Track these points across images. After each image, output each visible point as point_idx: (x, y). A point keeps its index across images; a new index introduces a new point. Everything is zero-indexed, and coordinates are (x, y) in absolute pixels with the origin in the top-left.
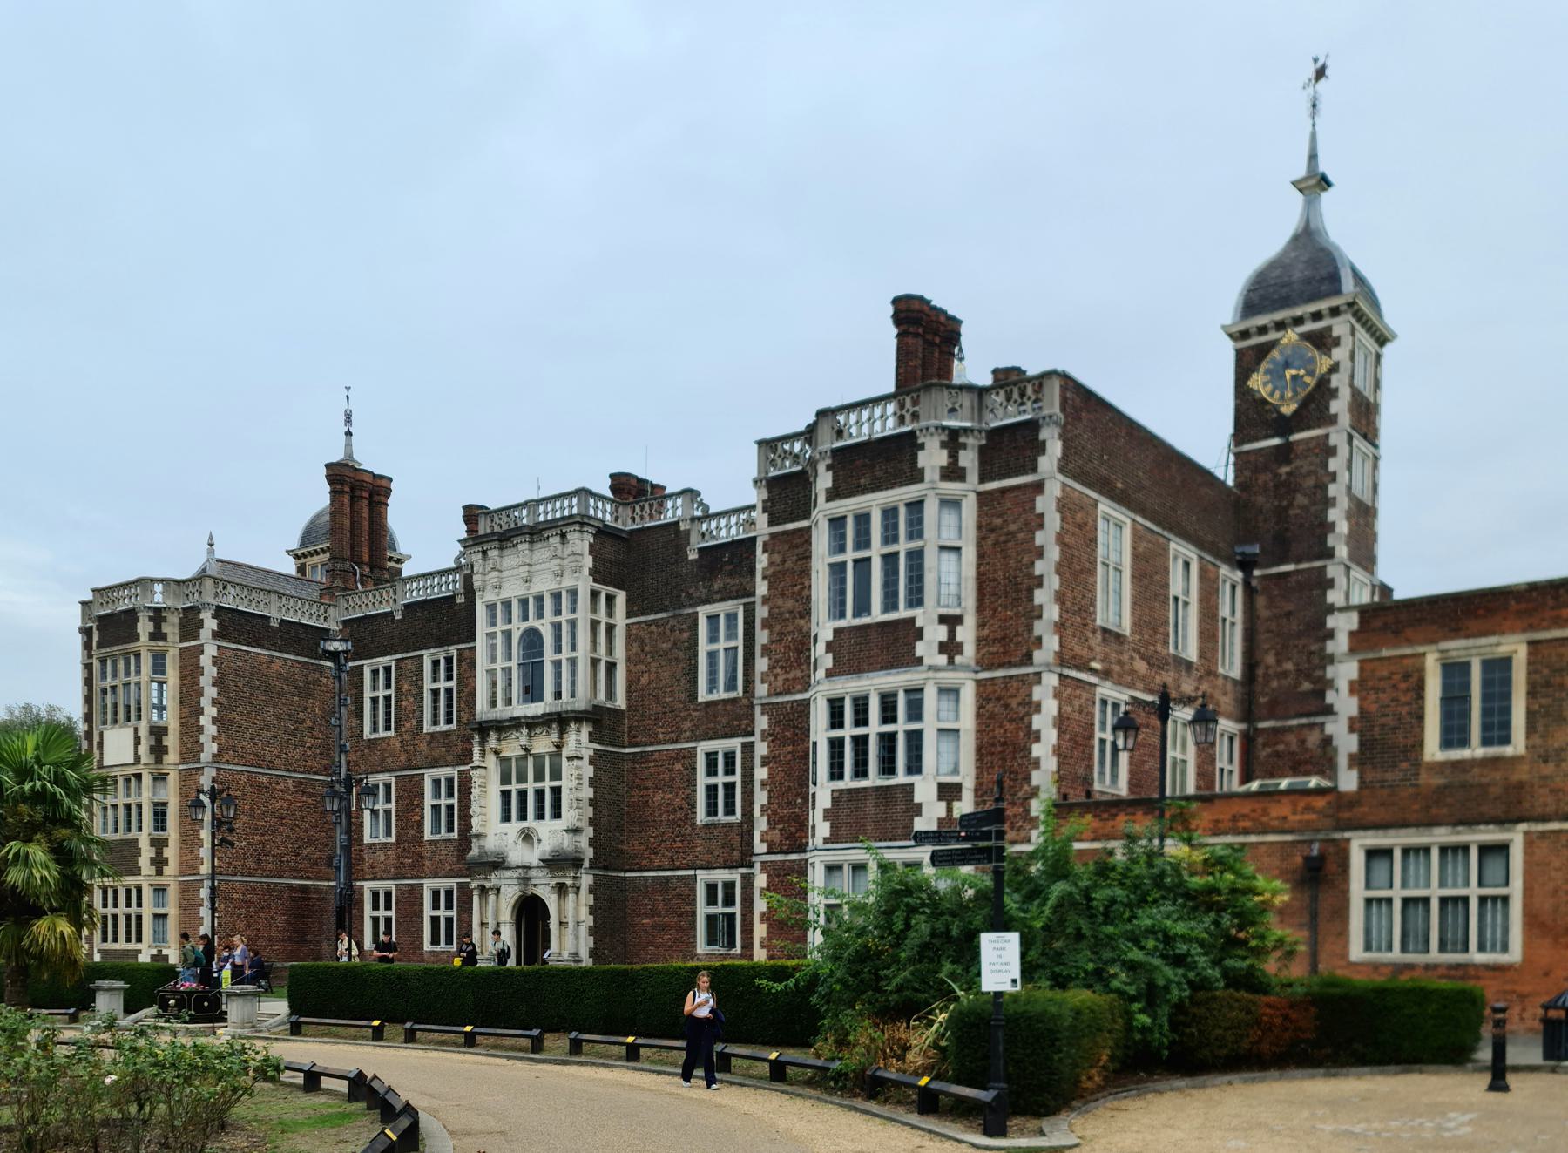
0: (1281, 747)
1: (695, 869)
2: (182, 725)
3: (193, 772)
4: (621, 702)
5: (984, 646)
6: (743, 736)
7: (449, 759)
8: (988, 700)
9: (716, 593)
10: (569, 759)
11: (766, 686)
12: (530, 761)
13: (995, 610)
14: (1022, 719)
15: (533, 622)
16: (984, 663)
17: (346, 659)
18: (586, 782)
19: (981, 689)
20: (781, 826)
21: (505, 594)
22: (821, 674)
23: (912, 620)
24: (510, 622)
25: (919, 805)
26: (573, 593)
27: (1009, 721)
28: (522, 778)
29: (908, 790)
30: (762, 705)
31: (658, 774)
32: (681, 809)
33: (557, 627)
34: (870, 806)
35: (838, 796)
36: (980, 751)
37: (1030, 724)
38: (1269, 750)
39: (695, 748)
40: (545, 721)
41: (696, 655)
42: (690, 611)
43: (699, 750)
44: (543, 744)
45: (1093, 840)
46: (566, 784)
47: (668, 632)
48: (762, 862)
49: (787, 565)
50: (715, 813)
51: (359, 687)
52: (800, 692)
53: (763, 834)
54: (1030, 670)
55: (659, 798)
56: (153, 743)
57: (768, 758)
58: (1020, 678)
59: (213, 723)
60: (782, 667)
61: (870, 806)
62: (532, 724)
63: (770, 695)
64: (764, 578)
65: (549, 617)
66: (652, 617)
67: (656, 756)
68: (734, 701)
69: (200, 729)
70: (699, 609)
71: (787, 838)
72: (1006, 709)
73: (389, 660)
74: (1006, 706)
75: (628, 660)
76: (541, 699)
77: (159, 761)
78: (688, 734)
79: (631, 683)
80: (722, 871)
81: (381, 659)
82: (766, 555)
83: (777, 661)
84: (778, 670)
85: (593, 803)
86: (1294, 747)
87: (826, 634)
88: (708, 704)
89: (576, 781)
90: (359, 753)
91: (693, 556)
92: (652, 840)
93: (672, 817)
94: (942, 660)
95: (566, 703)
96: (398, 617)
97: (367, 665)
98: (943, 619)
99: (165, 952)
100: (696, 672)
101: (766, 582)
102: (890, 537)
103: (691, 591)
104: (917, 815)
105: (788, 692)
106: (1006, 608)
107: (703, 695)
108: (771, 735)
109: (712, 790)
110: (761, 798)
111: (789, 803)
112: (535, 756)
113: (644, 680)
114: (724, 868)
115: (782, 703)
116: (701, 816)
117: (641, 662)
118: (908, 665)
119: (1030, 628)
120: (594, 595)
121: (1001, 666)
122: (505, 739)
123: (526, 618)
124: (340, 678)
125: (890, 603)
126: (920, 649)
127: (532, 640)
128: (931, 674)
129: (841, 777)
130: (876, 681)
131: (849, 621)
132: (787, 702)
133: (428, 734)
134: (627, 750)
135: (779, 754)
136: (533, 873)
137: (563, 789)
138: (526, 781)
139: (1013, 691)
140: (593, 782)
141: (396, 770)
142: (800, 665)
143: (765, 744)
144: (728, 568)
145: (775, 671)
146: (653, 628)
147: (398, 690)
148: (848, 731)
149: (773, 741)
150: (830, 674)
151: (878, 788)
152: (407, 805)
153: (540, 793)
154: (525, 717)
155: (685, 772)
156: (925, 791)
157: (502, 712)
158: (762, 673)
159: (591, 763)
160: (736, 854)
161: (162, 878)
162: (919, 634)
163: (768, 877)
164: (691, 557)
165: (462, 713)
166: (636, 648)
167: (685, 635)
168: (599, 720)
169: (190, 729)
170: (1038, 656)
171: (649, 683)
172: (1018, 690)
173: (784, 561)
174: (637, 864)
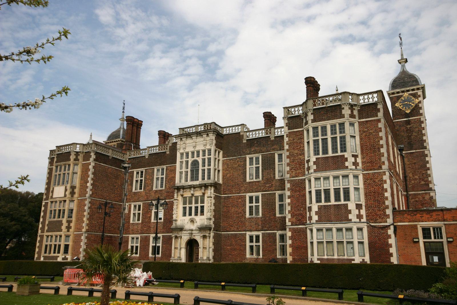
0: (417, 199)
1: (246, 231)
2: (81, 186)
3: (83, 200)
4: (221, 182)
5: (365, 164)
8: (367, 179)
10: (208, 197)
11: (289, 175)
12: (194, 198)
13: (367, 154)
14: (380, 185)
15: (195, 158)
16: (364, 169)
17: (129, 169)
18: (213, 204)
19: (365, 176)
20: (296, 217)
21: (187, 150)
23: (344, 155)
24: (188, 158)
25: (350, 210)
26: (210, 150)
27: (375, 186)
28: (191, 203)
29: (346, 206)
30: (288, 180)
32: (241, 213)
33: (204, 160)
34: (332, 210)
35: (320, 208)
36: (366, 195)
38: (413, 200)
39: (246, 195)
40: (200, 186)
41: (246, 168)
42: (244, 156)
43: (247, 196)
44: (198, 193)
46: (206, 205)
47: (236, 162)
48: (289, 228)
50: (252, 215)
51: (132, 177)
52: (301, 177)
53: (289, 219)
54: (381, 171)
55: (233, 209)
57: (290, 196)
58: (378, 173)
59: (91, 185)
60: (294, 169)
61: (332, 210)
62: (194, 187)
63: (290, 177)
64: (287, 144)
65: (201, 156)
66: (231, 158)
68: (259, 182)
70: (247, 156)
71: (298, 221)
72: (374, 182)
73: (143, 170)
74: (374, 181)
75: (223, 170)
76: (198, 180)
77: (72, 196)
78: (243, 191)
79: (223, 176)
82: (288, 138)
85: (214, 211)
86: (421, 199)
87: (313, 159)
88: (250, 182)
89: (209, 204)
90: (131, 196)
91: (245, 141)
94: (354, 167)
95: (206, 181)
96: (147, 157)
97: (135, 171)
98: (353, 156)
99: (67, 257)
100: (246, 173)
101: (288, 145)
102: (333, 131)
104: (349, 214)
105: (297, 176)
106: (371, 153)
107: (248, 180)
108: (291, 189)
109: (251, 208)
110: (288, 208)
111: (298, 210)
112: (195, 197)
113: (228, 175)
115: (295, 180)
116: (248, 215)
117: (227, 170)
119: (380, 159)
120: (216, 151)
121: (371, 170)
122: (185, 191)
123: (193, 157)
124: (126, 174)
125: (335, 150)
126: (347, 164)
127: (195, 164)
128: (351, 171)
129: (321, 202)
130: (332, 173)
132: (297, 179)
133: (155, 190)
134: (222, 196)
135: (294, 195)
136: (194, 232)
137: (205, 206)
138: (192, 204)
140: (214, 204)
141: (143, 201)
142: (300, 169)
143: (289, 192)
144: (256, 145)
145: (292, 171)
146: (231, 161)
147: (145, 178)
149: (292, 191)
151: (335, 205)
153: (196, 208)
154: (194, 185)
156: (351, 206)
157: (183, 183)
158: (287, 171)
159: (214, 199)
160: (260, 227)
161: (69, 233)
162: (346, 160)
163: (292, 233)
164: (244, 142)
165: (167, 185)
166: (226, 166)
167: (242, 163)
168: (216, 186)
169: (83, 187)
170: (383, 167)
172: (378, 177)
173: (294, 140)
174: (225, 230)
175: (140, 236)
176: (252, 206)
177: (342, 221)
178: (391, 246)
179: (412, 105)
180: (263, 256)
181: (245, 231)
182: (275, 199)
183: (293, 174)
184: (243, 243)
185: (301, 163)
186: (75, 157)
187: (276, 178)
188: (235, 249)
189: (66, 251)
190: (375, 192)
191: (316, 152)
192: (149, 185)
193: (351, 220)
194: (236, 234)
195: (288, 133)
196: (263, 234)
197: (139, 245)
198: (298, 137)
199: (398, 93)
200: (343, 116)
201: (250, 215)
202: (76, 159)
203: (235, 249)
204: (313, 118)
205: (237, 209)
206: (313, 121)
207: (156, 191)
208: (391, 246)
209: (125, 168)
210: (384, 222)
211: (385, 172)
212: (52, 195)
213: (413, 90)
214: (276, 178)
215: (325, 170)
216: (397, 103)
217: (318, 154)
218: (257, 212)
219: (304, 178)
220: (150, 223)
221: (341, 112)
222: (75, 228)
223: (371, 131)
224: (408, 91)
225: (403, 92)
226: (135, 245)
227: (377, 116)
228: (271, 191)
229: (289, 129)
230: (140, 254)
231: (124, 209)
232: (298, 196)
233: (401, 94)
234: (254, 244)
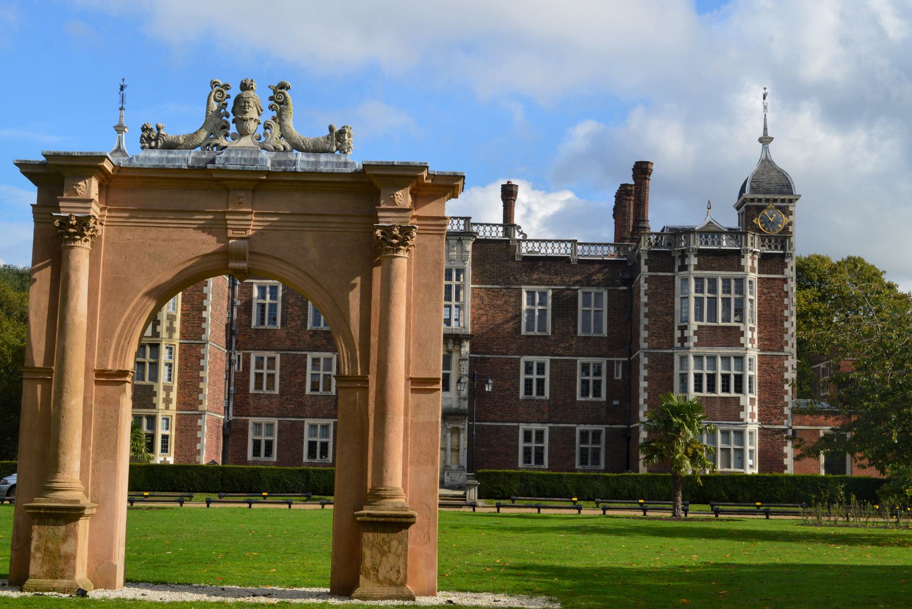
1: (519, 422)
6: (551, 356)
7: (329, 347)
8: (763, 364)
9: (534, 280)
11: (647, 344)
13: (766, 327)
14: (779, 373)
22: (692, 344)
23: (739, 327)
31: (493, 370)
37: (783, 376)
42: (517, 287)
45: (810, 425)
49: (658, 290)
50: (531, 394)
54: (783, 354)
56: (168, 325)
60: (656, 336)
61: (718, 405)
63: (649, 348)
66: (490, 286)
67: (492, 360)
69: (204, 320)
70: (522, 287)
74: (772, 367)
77: (171, 337)
78: (514, 350)
80: (537, 424)
81: (270, 281)
83: (654, 333)
84: (654, 338)
92: (488, 405)
93: (502, 394)
101: (647, 297)
103: (517, 277)
105: (659, 348)
113: (484, 319)
114: (538, 423)
115: (656, 353)
118: (736, 346)
119: (782, 338)
121: (769, 350)
125: (727, 319)
131: (705, 323)
132: (659, 353)
133: (311, 331)
139: (774, 362)
141: (281, 350)
142: (666, 337)
143: (646, 371)
144: (542, 269)
148: (706, 371)
149: (650, 370)
150: (696, 345)
152: (291, 372)
155: (512, 371)
160: (546, 416)
162: (742, 334)
166: (477, 301)
167: (512, 300)
171: (487, 321)
173: (657, 288)
175: (277, 422)
176: (531, 380)
177: (730, 421)
178: (785, 456)
179: (780, 226)
180: (549, 465)
181: (515, 422)
183: (655, 343)
184: (513, 443)
185: (669, 329)
187: (579, 335)
189: (165, 449)
190: (771, 383)
191: (699, 317)
192: (296, 318)
193: (742, 420)
194: (498, 427)
195: (647, 277)
196: (550, 428)
197: (275, 439)
198: (664, 285)
199: (760, 200)
200: (742, 269)
201: (526, 394)
204: (696, 263)
205: (501, 382)
206: (698, 267)
207: (315, 333)
208: (785, 456)
210: (780, 425)
211: (787, 356)
213: (783, 201)
214: (579, 335)
215: (711, 345)
216: (756, 218)
217: (702, 320)
218: (541, 392)
219: (671, 351)
220: (304, 395)
221: (740, 261)
222: (178, 403)
223: (773, 295)
224: (775, 201)
225: (767, 200)
226: (263, 438)
227: (783, 273)
228: (569, 356)
229: (649, 270)
230: (278, 457)
232: (660, 378)
233: (763, 204)
234: (533, 445)
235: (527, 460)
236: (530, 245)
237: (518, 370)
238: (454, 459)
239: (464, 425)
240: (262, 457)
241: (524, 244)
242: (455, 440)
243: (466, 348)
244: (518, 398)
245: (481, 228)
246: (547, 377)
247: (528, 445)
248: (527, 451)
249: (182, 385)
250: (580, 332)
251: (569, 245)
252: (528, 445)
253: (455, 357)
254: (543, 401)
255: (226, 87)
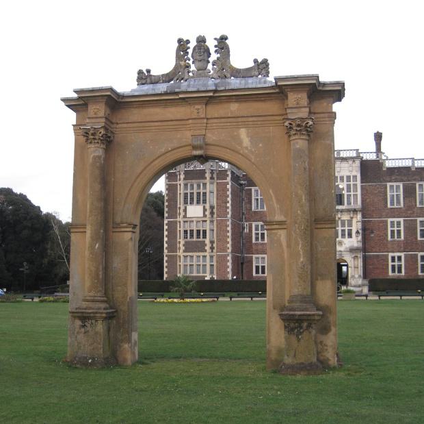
40: (348, 211)
41: (386, 195)
50: (394, 238)
65: (345, 183)
68: (400, 208)
77: (212, 217)
95: (352, 206)
107: (389, 206)
112: (342, 221)
160: (402, 249)
176: (394, 231)
182: (417, 224)
186: (210, 175)
188: (377, 268)
194: (378, 256)
201: (391, 238)
202: (212, 178)
203: (377, 268)
209: (241, 185)
212: (186, 214)
226: (260, 265)
231: (243, 228)
234: (396, 263)
235: (393, 271)
236: (390, 161)
237: (387, 226)
238: (356, 272)
239: (360, 255)
240: (260, 275)
241: (387, 161)
242: (356, 262)
243: (359, 216)
244: (387, 240)
245: (365, 154)
246: (402, 228)
247: (393, 264)
248: (393, 267)
249: (219, 240)
250: (418, 205)
251: (411, 160)
252: (393, 264)
253: (354, 221)
254: (400, 241)
255: (188, 42)
